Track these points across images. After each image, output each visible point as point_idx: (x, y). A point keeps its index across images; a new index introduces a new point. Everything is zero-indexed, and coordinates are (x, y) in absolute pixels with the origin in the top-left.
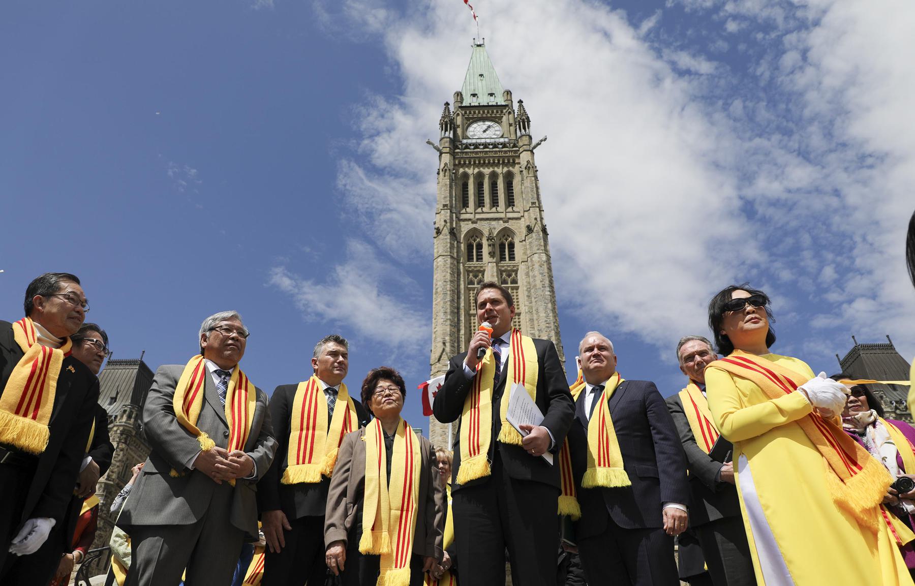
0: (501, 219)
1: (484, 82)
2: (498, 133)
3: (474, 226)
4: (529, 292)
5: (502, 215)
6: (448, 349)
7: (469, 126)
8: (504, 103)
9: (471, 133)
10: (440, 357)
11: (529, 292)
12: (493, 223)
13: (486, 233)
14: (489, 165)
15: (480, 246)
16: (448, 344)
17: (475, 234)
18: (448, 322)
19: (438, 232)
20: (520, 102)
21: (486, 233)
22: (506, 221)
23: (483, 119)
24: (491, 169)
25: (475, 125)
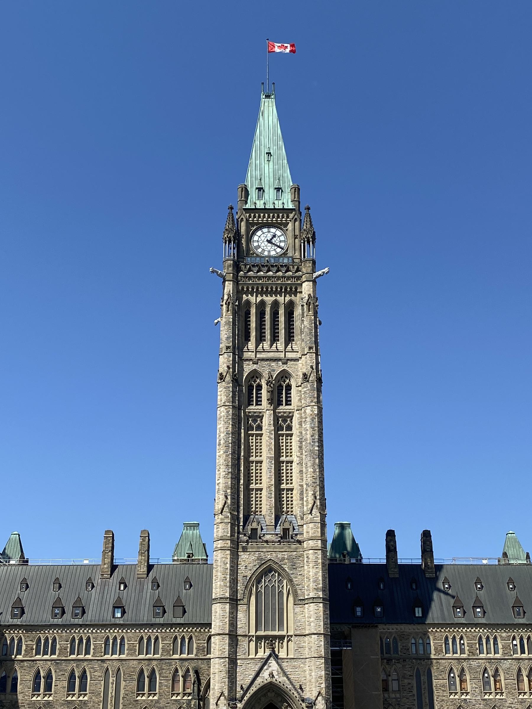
0: (280, 360)
1: (271, 163)
2: (282, 245)
3: (255, 367)
4: (301, 442)
5: (282, 355)
6: (229, 501)
7: (254, 233)
8: (291, 206)
9: (256, 244)
10: (223, 509)
11: (301, 442)
12: (273, 364)
13: (266, 375)
14: (271, 293)
15: (259, 387)
16: (229, 497)
17: (255, 375)
18: (230, 476)
19: (222, 377)
21: (266, 375)
22: (286, 361)
23: (269, 225)
24: (274, 298)
25: (259, 233)
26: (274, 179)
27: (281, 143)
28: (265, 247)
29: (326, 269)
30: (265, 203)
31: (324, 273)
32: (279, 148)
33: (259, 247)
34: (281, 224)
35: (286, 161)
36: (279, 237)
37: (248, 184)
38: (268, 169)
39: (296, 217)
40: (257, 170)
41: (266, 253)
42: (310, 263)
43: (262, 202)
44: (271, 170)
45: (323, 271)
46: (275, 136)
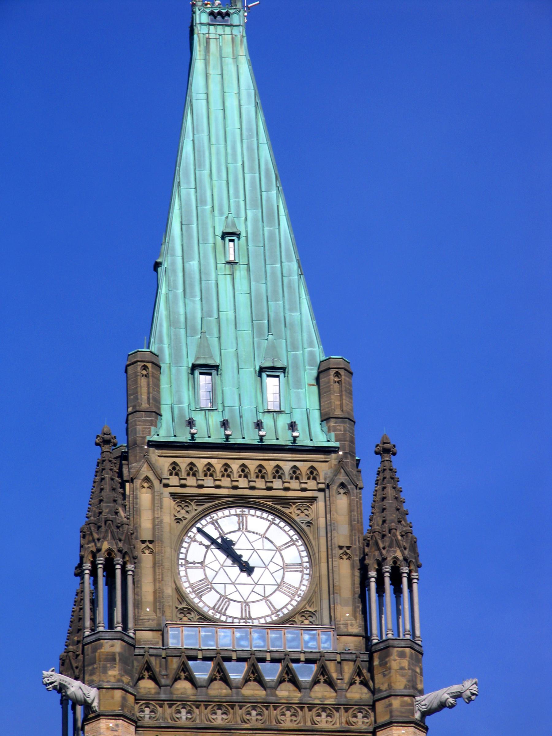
1: (241, 272)
8: (321, 439)
20: (386, 450)
26: (257, 332)
27: (275, 199)
28: (230, 589)
29: (468, 684)
30: (225, 424)
31: (457, 696)
32: (271, 218)
33: (207, 585)
34: (287, 502)
35: (295, 266)
36: (279, 550)
37: (161, 349)
38: (233, 296)
39: (342, 478)
40: (193, 296)
41: (234, 610)
42: (402, 655)
43: (215, 419)
44: (243, 299)
45: (456, 688)
46: (252, 170)
